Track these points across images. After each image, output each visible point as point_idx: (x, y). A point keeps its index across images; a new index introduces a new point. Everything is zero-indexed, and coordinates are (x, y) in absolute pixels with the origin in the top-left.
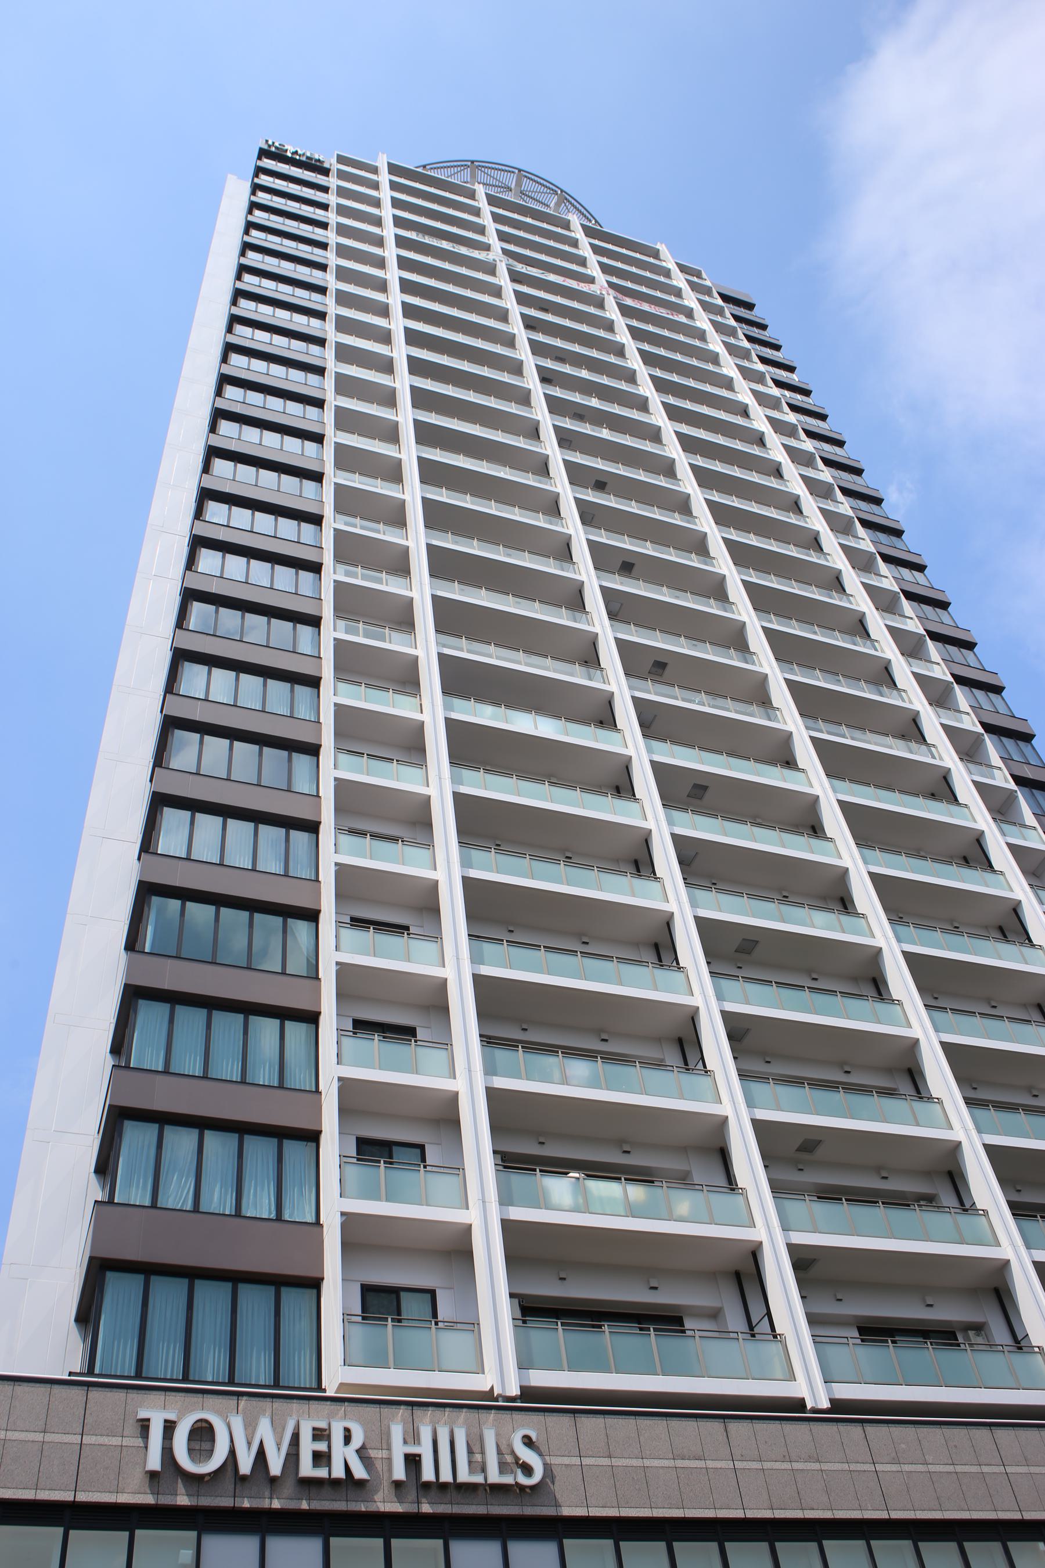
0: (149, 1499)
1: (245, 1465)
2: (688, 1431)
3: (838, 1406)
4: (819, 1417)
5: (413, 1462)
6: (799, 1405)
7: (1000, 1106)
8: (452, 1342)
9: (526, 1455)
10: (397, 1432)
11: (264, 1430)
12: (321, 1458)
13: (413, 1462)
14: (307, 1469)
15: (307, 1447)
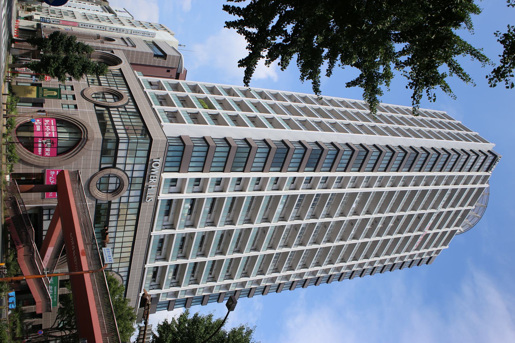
0: (150, 159)
1: (152, 170)
2: (150, 218)
3: (151, 236)
4: (150, 233)
5: (151, 187)
6: (152, 231)
7: (263, 259)
8: (167, 191)
9: (150, 200)
10: (154, 186)
11: (157, 172)
12: (152, 178)
13: (151, 187)
14: (151, 176)
15: (154, 176)
